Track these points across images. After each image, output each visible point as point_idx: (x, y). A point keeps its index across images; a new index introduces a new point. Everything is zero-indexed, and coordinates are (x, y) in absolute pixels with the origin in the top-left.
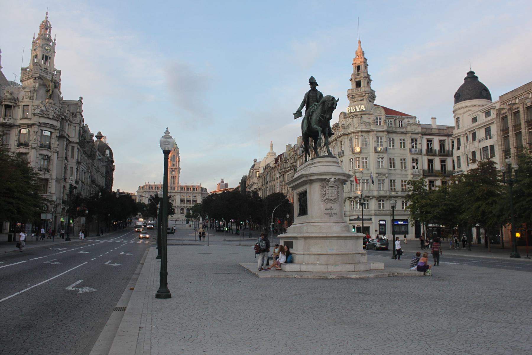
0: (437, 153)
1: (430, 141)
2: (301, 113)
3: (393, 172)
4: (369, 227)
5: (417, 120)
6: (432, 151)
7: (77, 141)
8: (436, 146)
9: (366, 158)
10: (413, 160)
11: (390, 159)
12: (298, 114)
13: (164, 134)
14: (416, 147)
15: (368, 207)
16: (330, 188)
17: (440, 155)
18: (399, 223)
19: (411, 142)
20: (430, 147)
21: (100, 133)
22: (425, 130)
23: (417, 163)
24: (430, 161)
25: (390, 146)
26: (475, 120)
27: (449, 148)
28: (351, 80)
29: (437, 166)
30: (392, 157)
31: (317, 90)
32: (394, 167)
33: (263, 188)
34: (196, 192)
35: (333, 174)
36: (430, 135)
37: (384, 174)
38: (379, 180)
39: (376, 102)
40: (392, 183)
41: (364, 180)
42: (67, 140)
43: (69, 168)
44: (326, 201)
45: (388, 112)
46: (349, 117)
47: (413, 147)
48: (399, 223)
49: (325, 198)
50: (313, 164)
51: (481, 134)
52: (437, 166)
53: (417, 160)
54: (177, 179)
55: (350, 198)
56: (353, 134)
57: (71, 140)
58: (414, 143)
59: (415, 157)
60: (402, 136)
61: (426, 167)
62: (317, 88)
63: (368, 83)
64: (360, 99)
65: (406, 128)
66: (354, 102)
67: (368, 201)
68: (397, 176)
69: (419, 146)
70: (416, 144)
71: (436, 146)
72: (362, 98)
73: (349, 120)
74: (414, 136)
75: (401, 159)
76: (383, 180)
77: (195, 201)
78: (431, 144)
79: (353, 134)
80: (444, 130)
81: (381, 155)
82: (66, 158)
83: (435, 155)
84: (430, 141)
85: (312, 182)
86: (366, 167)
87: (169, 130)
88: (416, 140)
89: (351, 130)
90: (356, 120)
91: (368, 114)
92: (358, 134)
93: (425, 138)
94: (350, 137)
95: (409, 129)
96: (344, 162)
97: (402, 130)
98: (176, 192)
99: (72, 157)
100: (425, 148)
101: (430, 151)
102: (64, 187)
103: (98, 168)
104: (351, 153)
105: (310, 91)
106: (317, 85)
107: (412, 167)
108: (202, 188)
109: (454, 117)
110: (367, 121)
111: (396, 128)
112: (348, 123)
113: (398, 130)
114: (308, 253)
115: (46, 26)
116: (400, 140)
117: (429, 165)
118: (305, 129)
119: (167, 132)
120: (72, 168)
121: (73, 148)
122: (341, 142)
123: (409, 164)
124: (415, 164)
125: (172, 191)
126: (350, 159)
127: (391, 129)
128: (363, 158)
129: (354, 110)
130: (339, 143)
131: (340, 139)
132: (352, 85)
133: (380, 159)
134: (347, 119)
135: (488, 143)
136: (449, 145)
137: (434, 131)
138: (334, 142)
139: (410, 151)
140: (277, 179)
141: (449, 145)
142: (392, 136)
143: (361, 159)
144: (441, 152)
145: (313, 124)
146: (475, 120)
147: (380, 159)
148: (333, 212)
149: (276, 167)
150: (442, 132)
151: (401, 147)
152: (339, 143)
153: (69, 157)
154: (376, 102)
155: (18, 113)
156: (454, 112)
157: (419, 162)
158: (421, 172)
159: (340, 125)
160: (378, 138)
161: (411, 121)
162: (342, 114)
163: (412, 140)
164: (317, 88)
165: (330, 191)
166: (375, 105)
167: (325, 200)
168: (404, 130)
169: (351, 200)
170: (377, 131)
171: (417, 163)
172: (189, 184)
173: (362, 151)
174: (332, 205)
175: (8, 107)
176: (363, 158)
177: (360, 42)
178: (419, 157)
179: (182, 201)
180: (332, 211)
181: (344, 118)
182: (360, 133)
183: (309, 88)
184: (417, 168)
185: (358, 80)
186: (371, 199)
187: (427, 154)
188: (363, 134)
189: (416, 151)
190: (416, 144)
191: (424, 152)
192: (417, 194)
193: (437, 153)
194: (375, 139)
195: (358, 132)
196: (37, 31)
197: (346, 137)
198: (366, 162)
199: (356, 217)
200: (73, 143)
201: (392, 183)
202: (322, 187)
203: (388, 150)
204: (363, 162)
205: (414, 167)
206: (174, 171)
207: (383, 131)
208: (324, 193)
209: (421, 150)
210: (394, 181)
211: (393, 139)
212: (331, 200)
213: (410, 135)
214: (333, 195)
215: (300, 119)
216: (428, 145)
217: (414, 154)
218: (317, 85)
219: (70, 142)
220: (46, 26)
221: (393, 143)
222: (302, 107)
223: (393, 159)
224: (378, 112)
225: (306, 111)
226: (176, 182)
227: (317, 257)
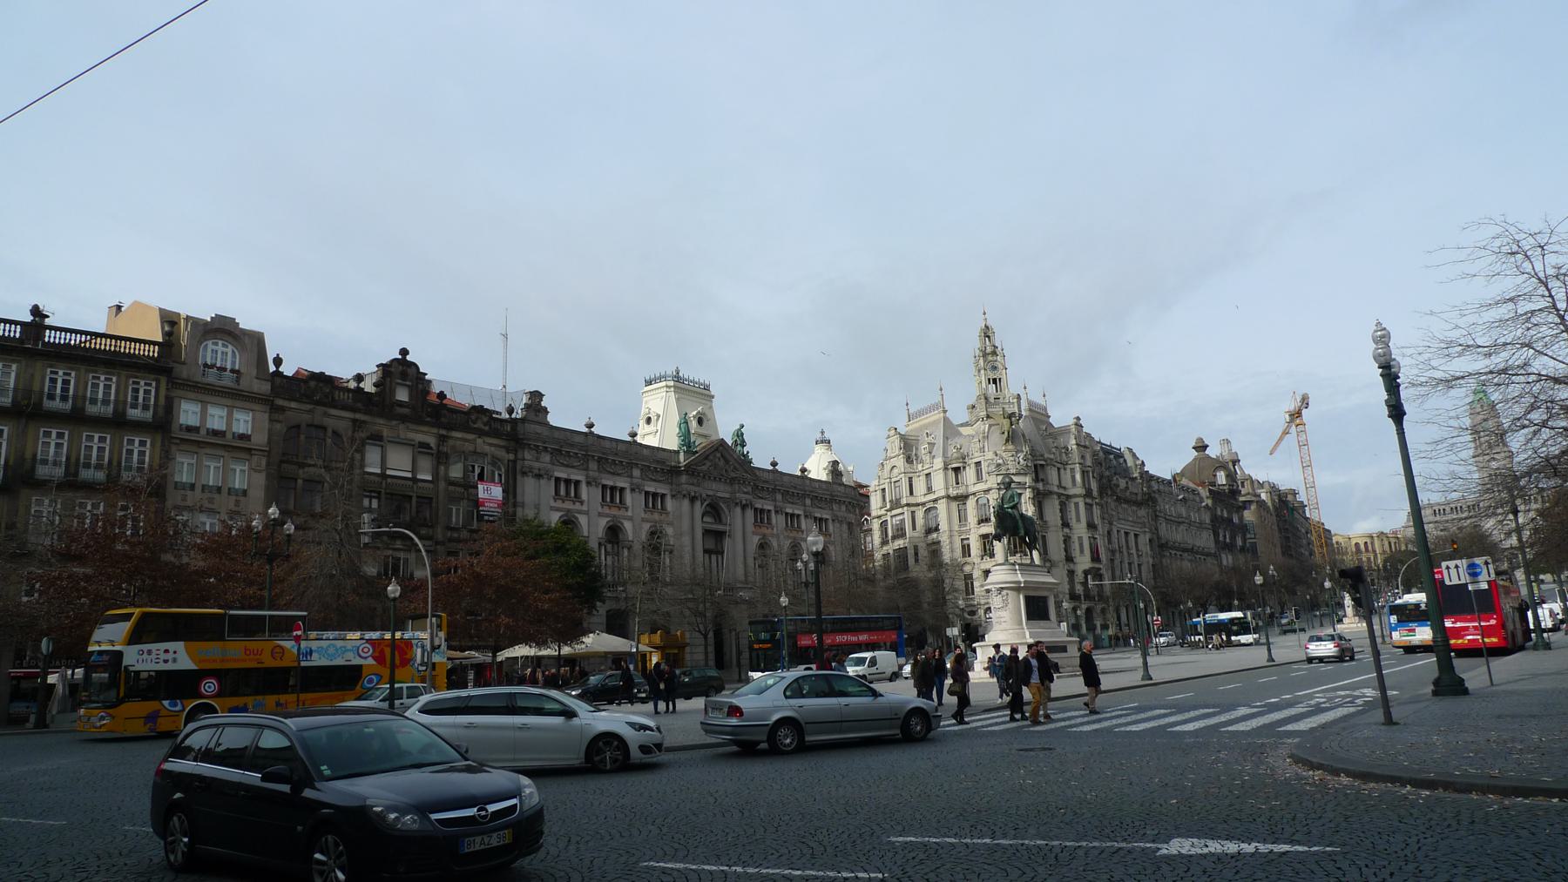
7: (1083, 492)
21: (1200, 440)
42: (1059, 495)
43: (1075, 538)
57: (1071, 492)
82: (1066, 524)
99: (1078, 520)
102: (1071, 573)
103: (1180, 516)
115: (987, 333)
120: (1080, 538)
121: (1077, 504)
153: (1073, 522)
155: (969, 474)
175: (956, 470)
196: (974, 343)
200: (1076, 496)
219: (1069, 497)
220: (987, 333)
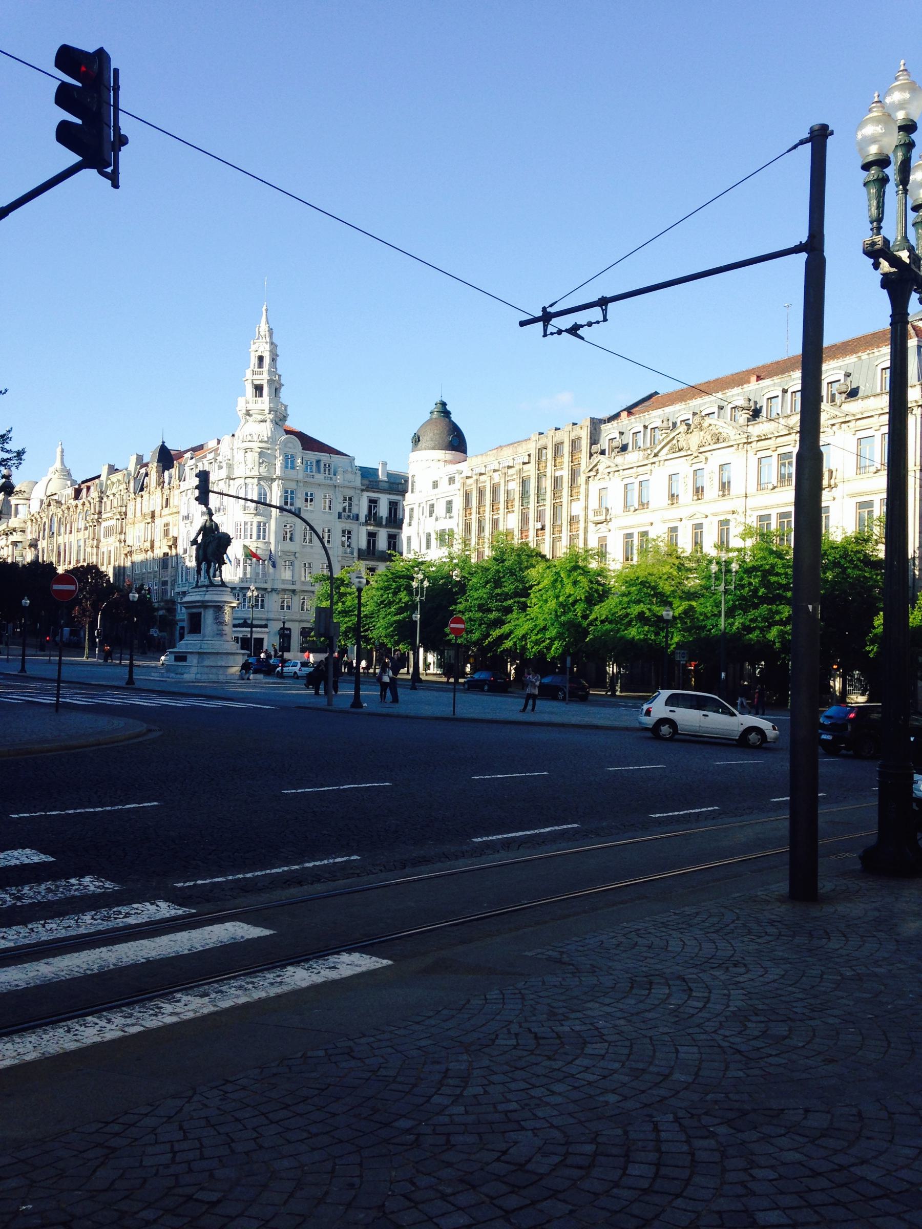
0: (384, 523)
1: (373, 502)
4: (262, 640)
8: (383, 511)
10: (344, 532)
14: (350, 511)
17: (386, 526)
19: (341, 500)
23: (349, 538)
24: (372, 535)
26: (435, 485)
47: (344, 510)
51: (440, 509)
53: (349, 532)
58: (347, 504)
61: (363, 544)
69: (355, 510)
70: (350, 505)
74: (350, 493)
78: (375, 507)
84: (373, 502)
85: (206, 607)
88: (350, 499)
93: (366, 495)
100: (364, 512)
101: (372, 517)
117: (369, 541)
124: (345, 539)
135: (446, 524)
139: (340, 517)
140: (78, 530)
144: (390, 522)
146: (435, 485)
157: (354, 536)
163: (345, 499)
171: (349, 538)
184: (349, 546)
189: (349, 516)
190: (350, 505)
191: (362, 519)
193: (384, 523)
202: (215, 612)
209: (358, 515)
211: (311, 495)
216: (370, 507)
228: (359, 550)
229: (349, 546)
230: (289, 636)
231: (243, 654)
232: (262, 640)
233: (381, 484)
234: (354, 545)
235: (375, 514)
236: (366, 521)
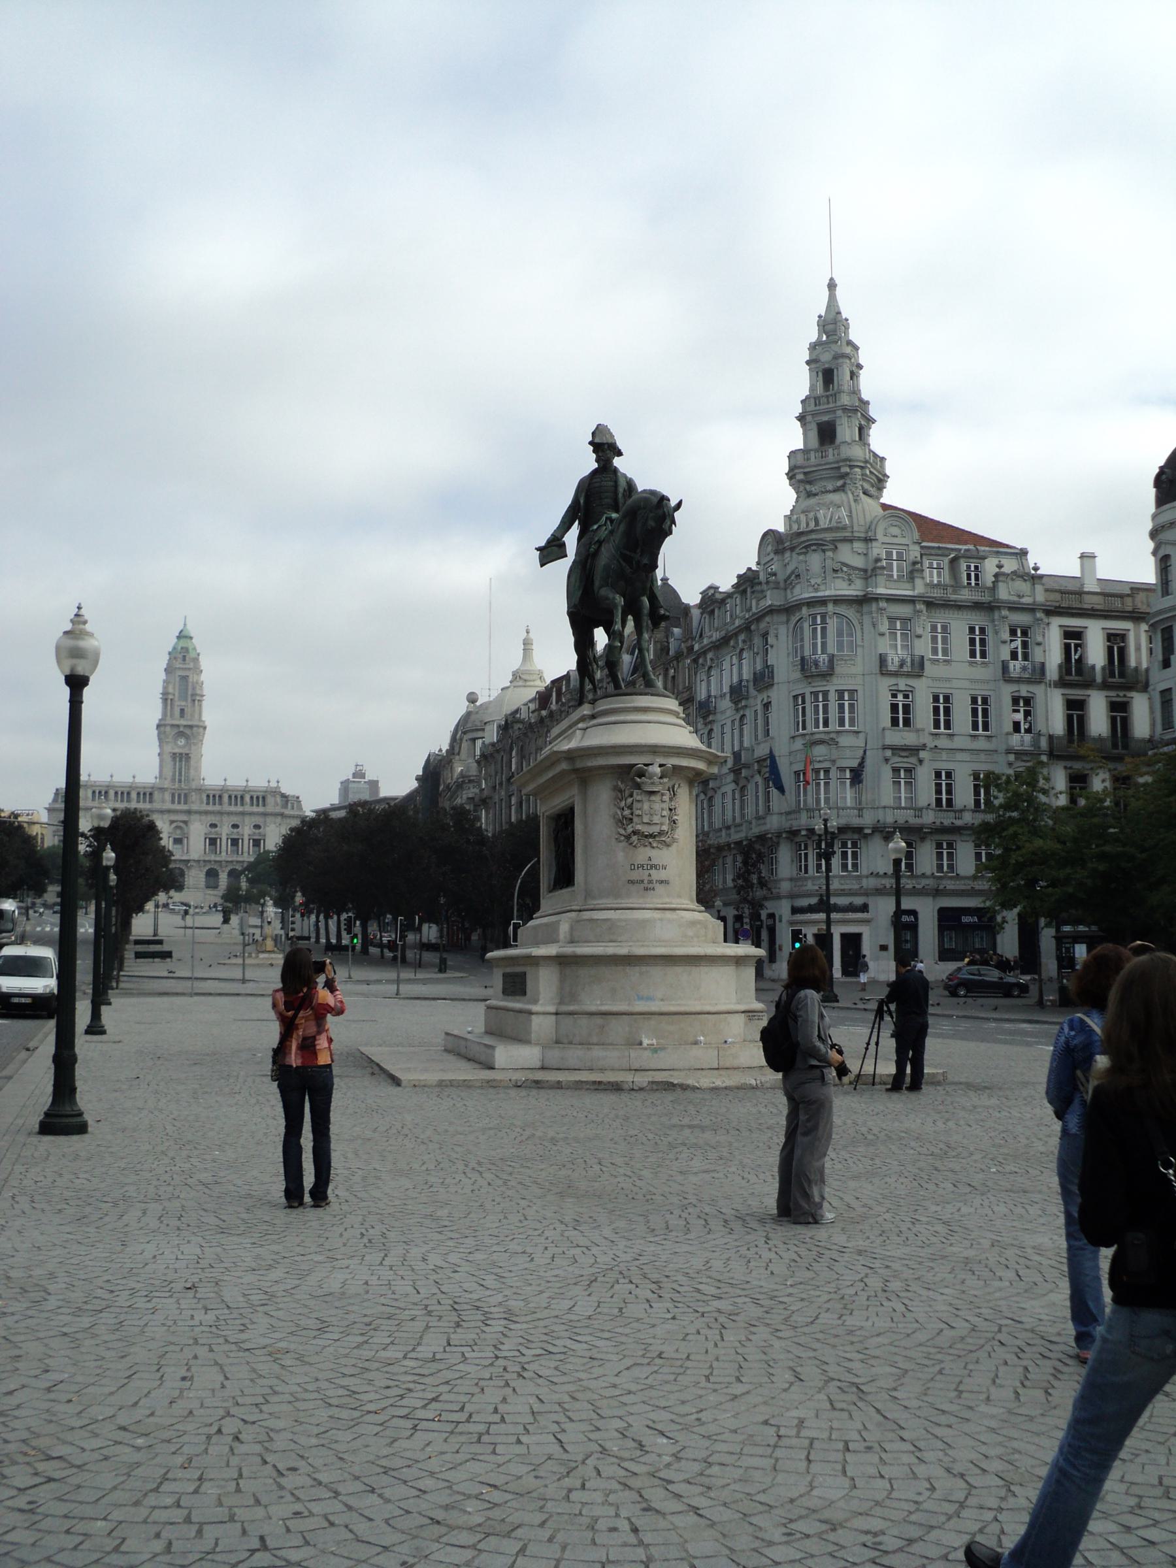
0: (1099, 679)
1: (1074, 636)
2: (564, 544)
3: (943, 743)
4: (858, 936)
5: (1031, 560)
6: (1080, 672)
8: (1096, 654)
9: (852, 692)
10: (1015, 701)
11: (936, 699)
12: (551, 551)
13: (68, 627)
14: (1026, 657)
15: (855, 866)
16: (644, 798)
17: (1105, 686)
18: (966, 919)
19: (1006, 636)
20: (1074, 657)
22: (1058, 596)
23: (1027, 714)
24: (1076, 707)
25: (935, 651)
27: (1139, 661)
28: (801, 418)
29: (1098, 722)
30: (942, 691)
31: (616, 470)
32: (948, 725)
33: (496, 798)
34: (261, 809)
35: (654, 750)
36: (1073, 615)
37: (913, 750)
38: (896, 770)
39: (890, 496)
40: (944, 780)
41: (842, 769)
44: (634, 838)
45: (929, 529)
46: (792, 549)
47: (1014, 655)
48: (966, 919)
49: (630, 829)
50: (593, 717)
52: (1098, 722)
53: (1028, 701)
54: (192, 762)
55: (793, 833)
56: (805, 610)
58: (1018, 643)
59: (1024, 690)
60: (978, 619)
61: (1058, 726)
62: (617, 462)
63: (861, 429)
64: (830, 487)
65: (994, 588)
66: (810, 495)
67: (855, 845)
68: (960, 756)
69: (1037, 655)
71: (1096, 654)
72: (840, 483)
73: (794, 561)
75: (974, 700)
76: (909, 771)
77: (257, 843)
79: (805, 610)
80: (1121, 596)
81: (902, 684)
83: (1089, 684)
84: (1074, 636)
86: (852, 723)
87: (82, 612)
88: (1025, 633)
89: (802, 593)
90: (815, 560)
91: (859, 539)
92: (822, 610)
94: (794, 619)
95: (1003, 593)
96: (774, 707)
97: (977, 597)
98: (189, 812)
100: (1053, 657)
101: (1074, 672)
104: (797, 675)
105: (594, 472)
106: (620, 454)
107: (1011, 729)
108: (283, 796)
109: (1154, 553)
110: (858, 562)
111: (956, 586)
112: (790, 569)
113: (965, 595)
114: (571, 1008)
116: (972, 630)
117: (1069, 719)
118: (576, 600)
119: (78, 619)
122: (765, 635)
123: (1005, 715)
124: (1019, 717)
125: (176, 807)
126: (795, 697)
127: (937, 594)
128: (840, 693)
129: (812, 525)
130: (757, 641)
131: (763, 625)
132: (805, 434)
133: (900, 697)
134: (787, 554)
136: (1138, 649)
137: (1089, 602)
138: (742, 637)
139: (1005, 667)
141: (1138, 649)
142: (941, 617)
143: (833, 696)
144: (1112, 675)
145: (597, 583)
147: (900, 697)
148: (656, 875)
149: (542, 720)
150: (1117, 604)
151: (973, 654)
152: (757, 641)
154: (890, 496)
156: (1153, 534)
158: (1044, 743)
159: (762, 577)
160: (892, 620)
161: (1010, 565)
162: (770, 539)
163: (1013, 632)
164: (617, 462)
165: (646, 806)
166: (885, 507)
167: (628, 837)
168: (986, 598)
169: (798, 839)
170: (891, 599)
172: (236, 781)
173: (838, 669)
174: (654, 853)
176: (840, 693)
177: (832, 286)
178: (1038, 690)
179: (213, 842)
180: (653, 872)
181: (776, 552)
182: (831, 607)
183: (589, 463)
185: (825, 418)
186: (866, 836)
187: (1062, 683)
188: (842, 609)
189: (1024, 669)
190: (1025, 645)
191: (1052, 672)
192: (1012, 821)
193: (1099, 679)
194: (884, 626)
195: (823, 602)
197: (783, 618)
198: (851, 706)
199: (814, 901)
201: (944, 780)
203: (927, 664)
204: (841, 707)
205: (1016, 726)
206: (181, 734)
207: (911, 601)
208: (627, 812)
210: (949, 775)
211: (945, 629)
212: (652, 836)
213: (1005, 612)
214: (656, 819)
215: (562, 568)
216: (1067, 648)
217: (1019, 681)
218: (620, 454)
221: (945, 641)
222: (565, 525)
223: (947, 699)
224: (895, 531)
225: (579, 539)
226: (192, 772)
227: (599, 1020)
228: (1051, 737)
229: (1028, 731)
230: (913, 927)
231: (739, 961)
232: (858, 936)
233: (1087, 598)
234: (1040, 726)
235: (1080, 661)
236: (1061, 678)
